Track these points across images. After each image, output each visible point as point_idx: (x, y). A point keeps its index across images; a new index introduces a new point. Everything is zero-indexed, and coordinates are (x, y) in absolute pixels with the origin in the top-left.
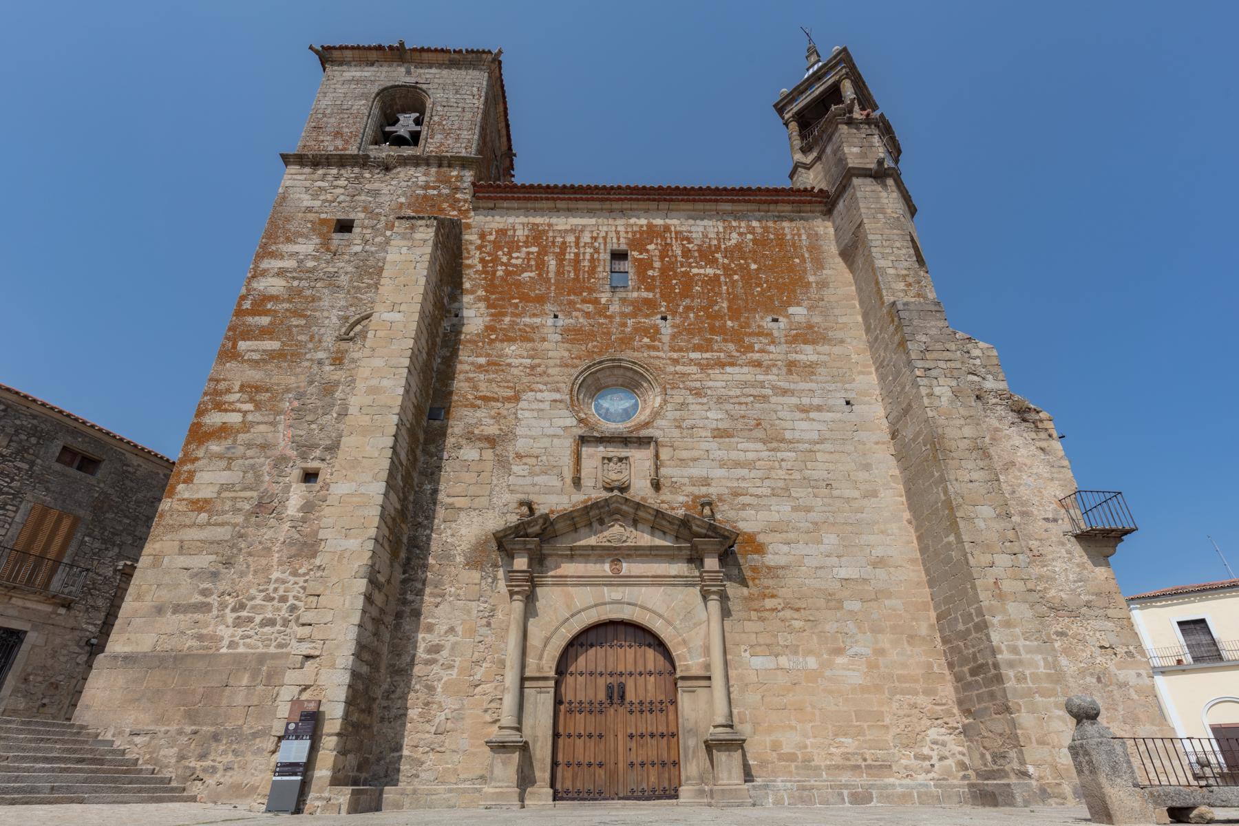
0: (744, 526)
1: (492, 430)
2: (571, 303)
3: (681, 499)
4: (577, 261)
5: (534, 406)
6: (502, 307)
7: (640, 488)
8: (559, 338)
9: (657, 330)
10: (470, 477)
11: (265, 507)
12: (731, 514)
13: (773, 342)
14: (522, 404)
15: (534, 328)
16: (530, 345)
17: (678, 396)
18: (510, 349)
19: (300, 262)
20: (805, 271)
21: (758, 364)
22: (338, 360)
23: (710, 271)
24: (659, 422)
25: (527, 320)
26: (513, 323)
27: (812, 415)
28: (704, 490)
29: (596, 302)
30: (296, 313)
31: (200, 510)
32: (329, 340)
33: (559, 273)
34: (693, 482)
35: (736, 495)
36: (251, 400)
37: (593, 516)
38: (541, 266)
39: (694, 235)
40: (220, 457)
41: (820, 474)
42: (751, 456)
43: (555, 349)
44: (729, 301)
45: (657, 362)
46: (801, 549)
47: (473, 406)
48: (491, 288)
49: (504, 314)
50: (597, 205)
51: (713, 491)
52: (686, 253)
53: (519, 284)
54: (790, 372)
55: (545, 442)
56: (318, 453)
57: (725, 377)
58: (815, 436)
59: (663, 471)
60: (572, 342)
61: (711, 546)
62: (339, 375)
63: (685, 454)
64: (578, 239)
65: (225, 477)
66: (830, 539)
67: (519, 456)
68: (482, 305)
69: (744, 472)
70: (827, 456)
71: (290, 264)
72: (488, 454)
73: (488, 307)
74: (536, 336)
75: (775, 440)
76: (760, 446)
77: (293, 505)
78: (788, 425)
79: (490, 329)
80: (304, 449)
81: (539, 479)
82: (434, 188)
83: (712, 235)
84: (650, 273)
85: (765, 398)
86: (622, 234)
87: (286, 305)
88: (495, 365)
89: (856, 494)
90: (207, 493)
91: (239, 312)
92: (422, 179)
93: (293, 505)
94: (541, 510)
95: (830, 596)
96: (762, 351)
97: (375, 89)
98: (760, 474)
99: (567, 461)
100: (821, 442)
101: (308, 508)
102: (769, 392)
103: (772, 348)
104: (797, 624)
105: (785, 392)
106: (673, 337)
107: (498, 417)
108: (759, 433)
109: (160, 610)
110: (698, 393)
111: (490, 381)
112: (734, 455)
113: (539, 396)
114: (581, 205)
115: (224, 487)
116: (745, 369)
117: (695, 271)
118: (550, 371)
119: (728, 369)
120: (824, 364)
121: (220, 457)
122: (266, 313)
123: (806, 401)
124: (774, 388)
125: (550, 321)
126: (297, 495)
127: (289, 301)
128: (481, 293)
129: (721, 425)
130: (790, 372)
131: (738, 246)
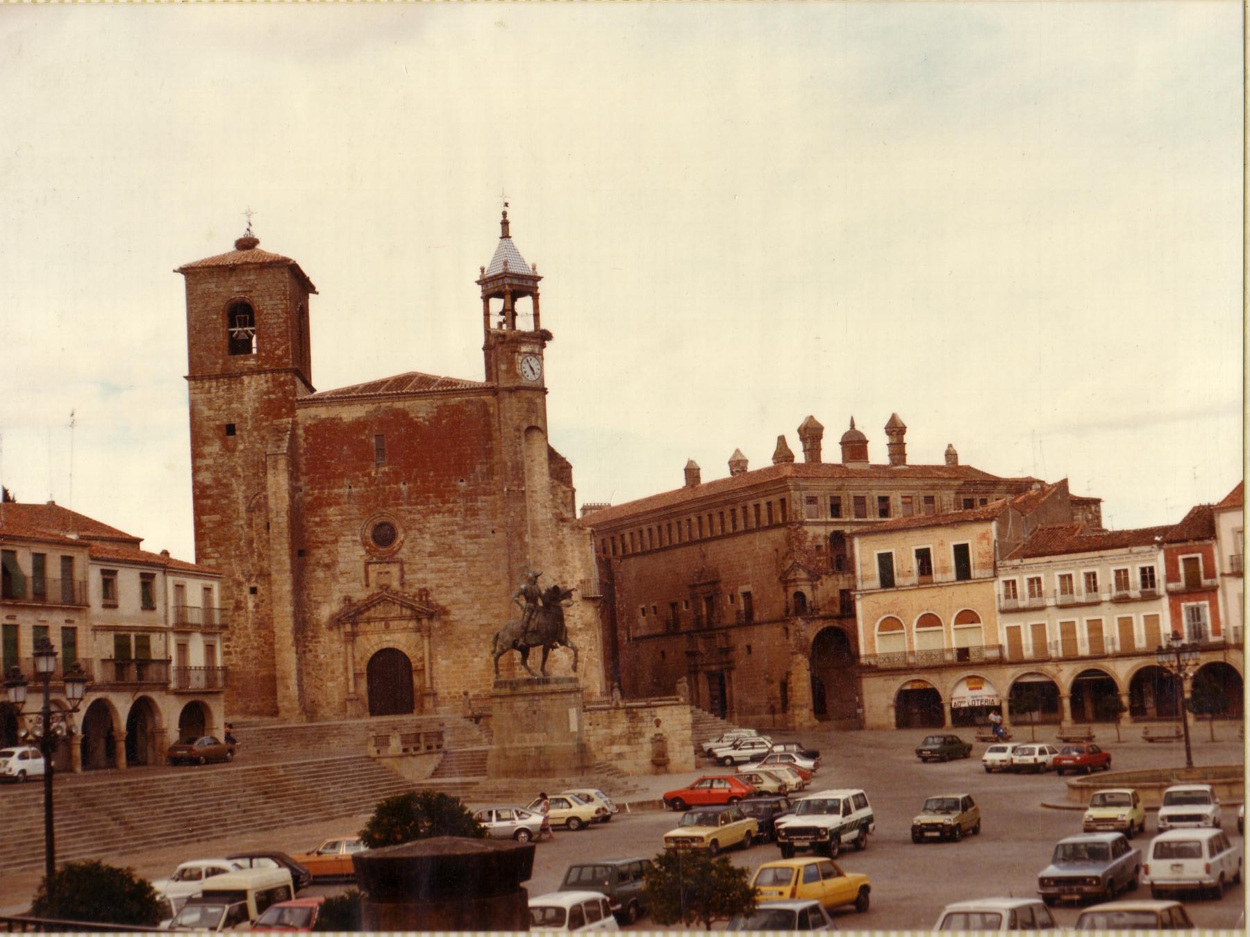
0: (442, 603)
1: (327, 560)
7: (395, 585)
10: (321, 586)
11: (238, 607)
15: (340, 496)
17: (413, 533)
18: (331, 511)
19: (215, 459)
21: (451, 511)
24: (404, 550)
25: (336, 491)
26: (330, 494)
29: (369, 475)
32: (243, 514)
34: (419, 581)
41: (475, 574)
46: (465, 612)
51: (428, 586)
56: (254, 579)
58: (475, 553)
61: (425, 613)
63: (414, 567)
67: (342, 574)
71: (209, 461)
74: (342, 501)
77: (251, 605)
81: (352, 585)
82: (273, 393)
85: (452, 533)
88: (324, 522)
89: (489, 583)
92: (264, 387)
93: (251, 605)
94: (355, 600)
99: (362, 575)
100: (479, 555)
101: (257, 606)
107: (330, 553)
110: (419, 530)
122: (209, 497)
124: (457, 524)
125: (347, 490)
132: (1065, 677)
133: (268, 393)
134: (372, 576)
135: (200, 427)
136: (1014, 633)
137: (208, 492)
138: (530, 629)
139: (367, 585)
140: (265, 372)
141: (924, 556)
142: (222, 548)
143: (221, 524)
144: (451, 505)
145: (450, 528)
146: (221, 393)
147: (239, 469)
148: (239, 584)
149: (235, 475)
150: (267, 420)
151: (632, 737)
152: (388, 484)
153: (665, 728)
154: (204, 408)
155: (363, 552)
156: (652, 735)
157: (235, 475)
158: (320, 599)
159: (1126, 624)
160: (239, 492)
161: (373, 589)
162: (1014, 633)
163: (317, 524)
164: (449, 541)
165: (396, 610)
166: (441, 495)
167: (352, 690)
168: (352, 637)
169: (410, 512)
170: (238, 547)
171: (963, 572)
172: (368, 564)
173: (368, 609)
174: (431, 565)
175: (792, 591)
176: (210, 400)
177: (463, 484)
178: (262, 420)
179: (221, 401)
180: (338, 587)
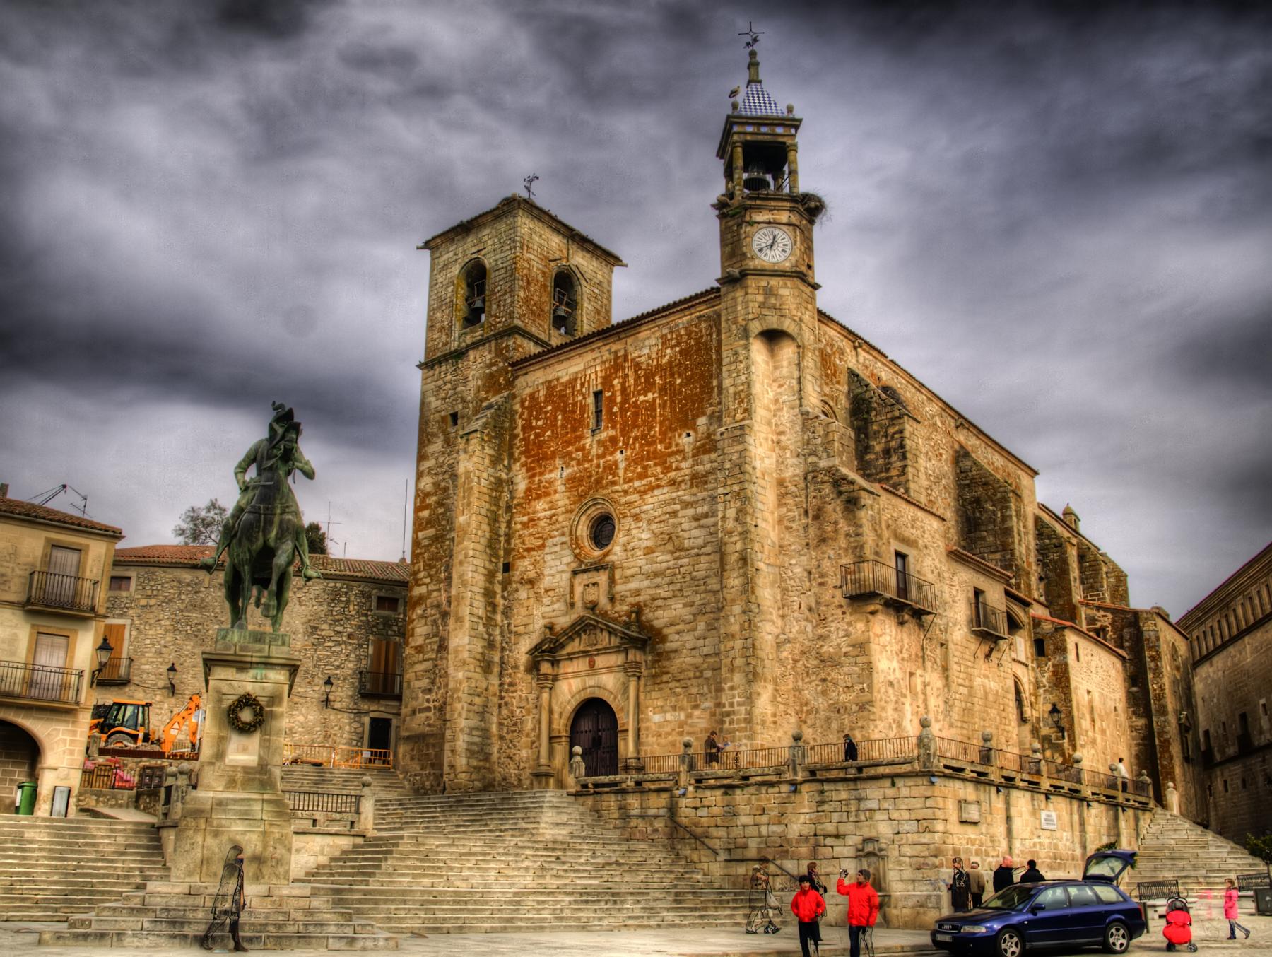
0: (657, 624)
1: (532, 574)
2: (569, 453)
3: (625, 608)
4: (574, 412)
5: (554, 549)
6: (533, 469)
7: (603, 601)
8: (561, 488)
9: (617, 468)
12: (651, 615)
13: (684, 459)
14: (547, 550)
15: (551, 482)
16: (548, 499)
18: (540, 505)
19: (437, 459)
20: (711, 376)
21: (673, 483)
23: (650, 396)
24: (617, 549)
25: (547, 476)
26: (540, 481)
27: (703, 522)
28: (637, 599)
29: (582, 449)
31: (419, 652)
33: (563, 427)
35: (654, 599)
36: (430, 576)
37: (580, 628)
38: (553, 426)
39: (643, 359)
40: (421, 617)
42: (664, 565)
43: (562, 498)
44: (661, 424)
45: (615, 496)
46: (686, 637)
47: (523, 557)
48: (526, 452)
49: (533, 476)
50: (583, 350)
51: (641, 598)
52: (637, 378)
53: (540, 445)
54: (692, 486)
55: (558, 576)
57: (654, 500)
58: (700, 541)
59: (618, 588)
63: (629, 572)
64: (573, 387)
67: (546, 591)
68: (524, 470)
69: (659, 580)
70: (707, 558)
72: (531, 592)
73: (528, 471)
74: (551, 490)
76: (668, 557)
78: (686, 535)
79: (529, 490)
81: (556, 606)
82: (494, 364)
83: (654, 356)
84: (615, 409)
86: (599, 374)
87: (435, 498)
94: (557, 629)
96: (678, 469)
97: (456, 270)
98: (667, 580)
100: (705, 545)
102: (678, 507)
103: (683, 465)
104: (678, 690)
105: (686, 505)
106: (626, 470)
107: (535, 563)
108: (670, 547)
109: (414, 712)
110: (637, 518)
111: (530, 535)
112: (656, 567)
113: (556, 540)
114: (573, 354)
115: (427, 637)
116: (665, 490)
117: (642, 398)
118: (560, 519)
119: (656, 492)
121: (421, 617)
123: (699, 510)
127: (435, 494)
128: (523, 459)
129: (649, 543)
130: (692, 486)
131: (670, 362)
133: (492, 364)
134: (579, 590)
137: (428, 501)
139: (572, 605)
140: (488, 340)
143: (436, 539)
144: (672, 474)
145: (669, 509)
150: (486, 399)
152: (603, 456)
154: (433, 399)
155: (570, 558)
156: (858, 840)
158: (521, 629)
161: (579, 611)
165: (604, 639)
166: (662, 460)
167: (543, 761)
168: (548, 682)
169: (626, 492)
172: (575, 573)
173: (571, 639)
177: (691, 439)
178: (481, 401)
179: (449, 386)
180: (544, 609)
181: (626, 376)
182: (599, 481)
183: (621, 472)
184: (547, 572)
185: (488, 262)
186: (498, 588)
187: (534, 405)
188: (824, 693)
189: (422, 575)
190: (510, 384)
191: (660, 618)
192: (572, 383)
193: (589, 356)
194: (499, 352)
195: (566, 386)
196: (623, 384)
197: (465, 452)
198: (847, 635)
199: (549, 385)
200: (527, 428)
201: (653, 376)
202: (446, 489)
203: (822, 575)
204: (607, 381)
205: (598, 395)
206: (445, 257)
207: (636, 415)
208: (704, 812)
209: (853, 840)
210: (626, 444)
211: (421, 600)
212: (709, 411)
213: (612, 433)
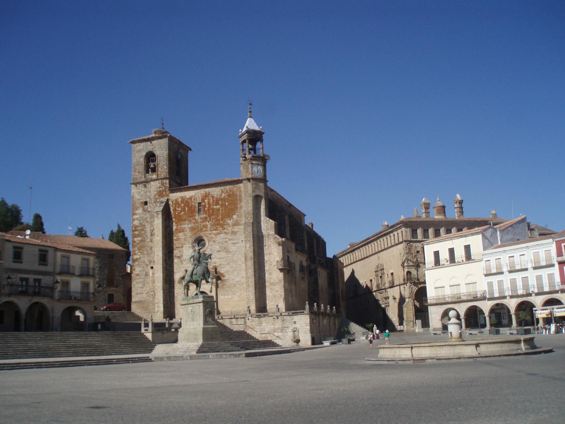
0: (222, 272)
1: (179, 255)
2: (191, 220)
11: (147, 275)
13: (229, 226)
15: (184, 228)
17: (211, 243)
18: (181, 235)
21: (226, 233)
22: (151, 241)
23: (218, 207)
24: (208, 250)
25: (183, 226)
29: (195, 219)
30: (143, 230)
33: (188, 212)
35: (220, 265)
39: (215, 195)
41: (234, 259)
43: (188, 233)
44: (222, 215)
49: (178, 225)
51: (216, 265)
52: (213, 201)
53: (180, 216)
58: (235, 250)
60: (191, 231)
62: (152, 245)
64: (191, 200)
65: (140, 269)
66: (236, 273)
69: (222, 260)
71: (137, 216)
72: (179, 260)
75: (228, 252)
79: (176, 229)
80: (150, 262)
85: (226, 242)
90: (138, 273)
91: (133, 231)
95: (234, 284)
97: (144, 154)
101: (153, 274)
105: (230, 240)
107: (180, 252)
108: (225, 251)
109: (137, 294)
110: (214, 242)
115: (140, 271)
120: (238, 231)
122: (137, 230)
123: (234, 242)
126: (151, 272)
132: (512, 304)
133: (160, 188)
135: (135, 203)
136: (490, 284)
138: (195, 272)
140: (159, 179)
141: (451, 251)
142: (141, 251)
143: (141, 241)
144: (225, 231)
146: (143, 189)
147: (148, 219)
148: (147, 265)
149: (147, 222)
151: (283, 329)
152: (202, 222)
153: (298, 326)
156: (292, 328)
157: (147, 222)
159: (539, 278)
160: (148, 229)
162: (490, 284)
163: (176, 240)
164: (224, 246)
166: (222, 226)
169: (210, 234)
170: (147, 250)
171: (468, 257)
174: (218, 256)
175: (406, 270)
176: (139, 192)
178: (157, 199)
181: (209, 200)
182: (201, 230)
183: (209, 228)
184: (184, 254)
185: (157, 153)
186: (167, 258)
187: (177, 203)
188: (271, 292)
189: (137, 252)
190: (167, 195)
191: (221, 270)
192: (191, 198)
193: (197, 191)
194: (163, 184)
195: (188, 199)
196: (208, 202)
197: (157, 217)
198: (277, 278)
199: (182, 198)
200: (175, 210)
201: (219, 201)
202: (144, 226)
203: (271, 262)
204: (203, 200)
205: (199, 204)
206: (139, 147)
207: (213, 212)
208: (254, 323)
209: (291, 328)
210: (210, 220)
211: (137, 260)
212: (237, 214)
213: (205, 216)
